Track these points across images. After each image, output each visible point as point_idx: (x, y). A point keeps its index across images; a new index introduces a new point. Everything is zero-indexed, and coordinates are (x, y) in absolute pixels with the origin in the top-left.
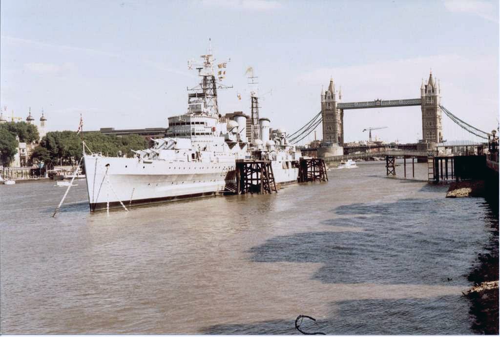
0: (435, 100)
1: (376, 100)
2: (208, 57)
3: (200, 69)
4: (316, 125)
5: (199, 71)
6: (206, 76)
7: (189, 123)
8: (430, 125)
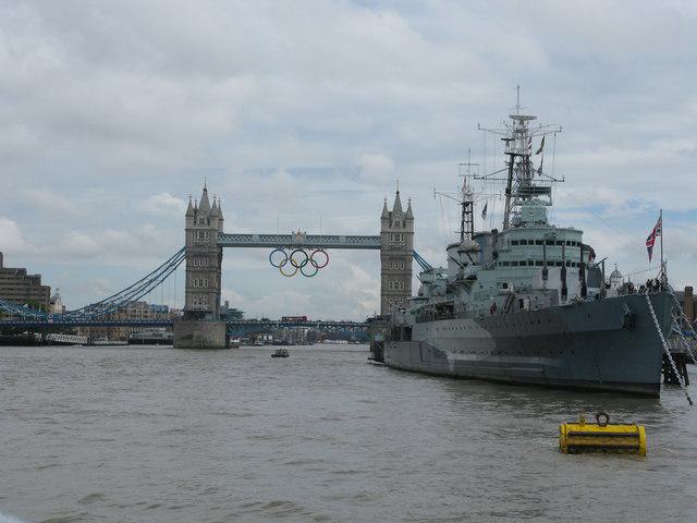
0: (409, 242)
1: (296, 233)
2: (522, 119)
3: (507, 140)
4: (165, 274)
5: (507, 145)
6: (513, 155)
7: (559, 243)
8: (396, 287)
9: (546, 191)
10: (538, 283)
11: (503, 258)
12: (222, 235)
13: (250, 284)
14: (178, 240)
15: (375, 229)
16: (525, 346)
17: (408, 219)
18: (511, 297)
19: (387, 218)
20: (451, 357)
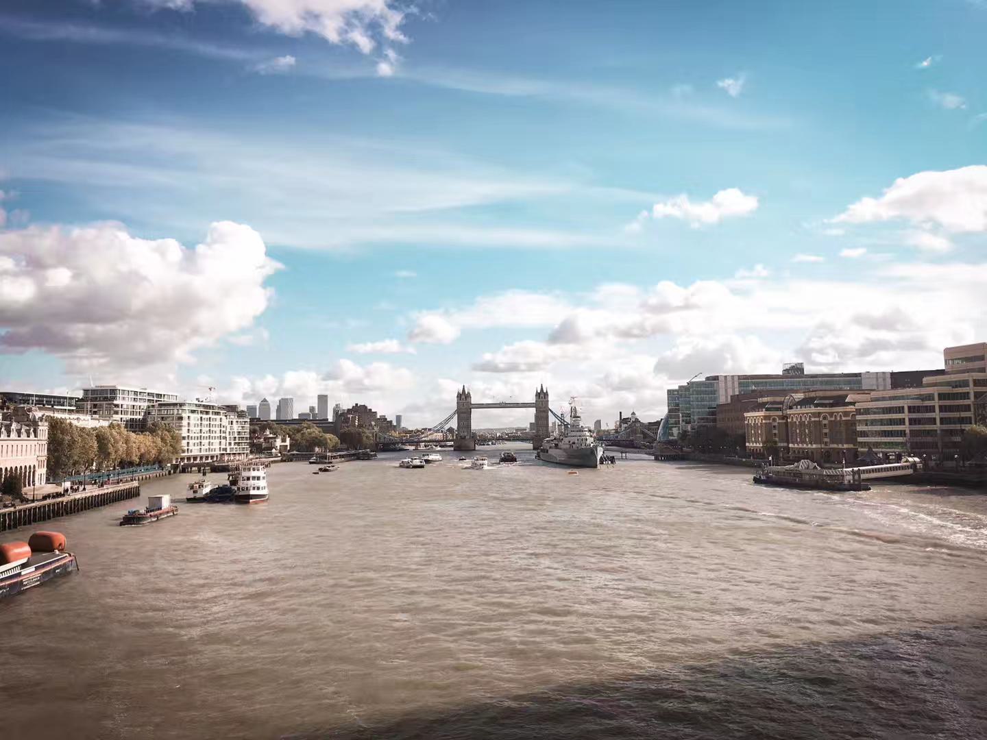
9: (579, 417)
10: (576, 442)
11: (569, 435)
12: (471, 404)
13: (480, 422)
14: (454, 406)
15: (532, 399)
16: (575, 457)
17: (546, 394)
18: (570, 445)
19: (538, 395)
20: (558, 459)
